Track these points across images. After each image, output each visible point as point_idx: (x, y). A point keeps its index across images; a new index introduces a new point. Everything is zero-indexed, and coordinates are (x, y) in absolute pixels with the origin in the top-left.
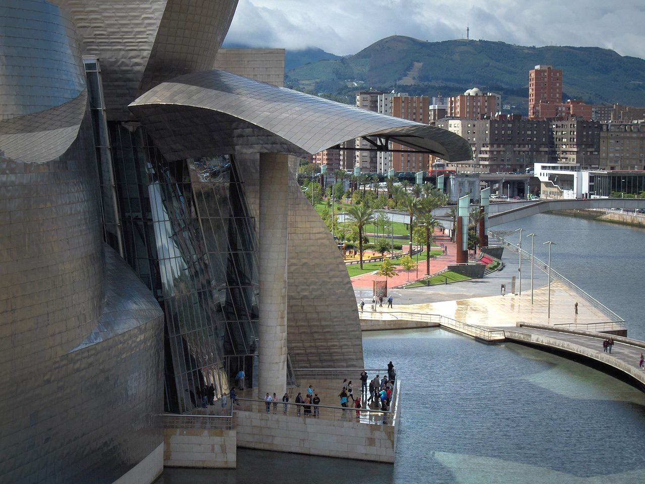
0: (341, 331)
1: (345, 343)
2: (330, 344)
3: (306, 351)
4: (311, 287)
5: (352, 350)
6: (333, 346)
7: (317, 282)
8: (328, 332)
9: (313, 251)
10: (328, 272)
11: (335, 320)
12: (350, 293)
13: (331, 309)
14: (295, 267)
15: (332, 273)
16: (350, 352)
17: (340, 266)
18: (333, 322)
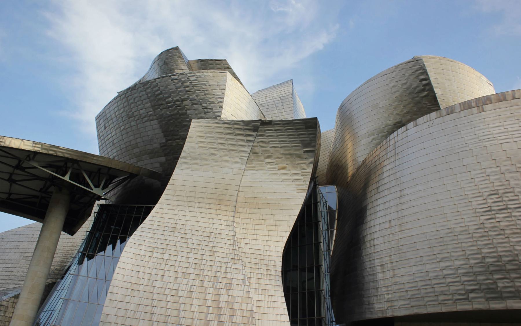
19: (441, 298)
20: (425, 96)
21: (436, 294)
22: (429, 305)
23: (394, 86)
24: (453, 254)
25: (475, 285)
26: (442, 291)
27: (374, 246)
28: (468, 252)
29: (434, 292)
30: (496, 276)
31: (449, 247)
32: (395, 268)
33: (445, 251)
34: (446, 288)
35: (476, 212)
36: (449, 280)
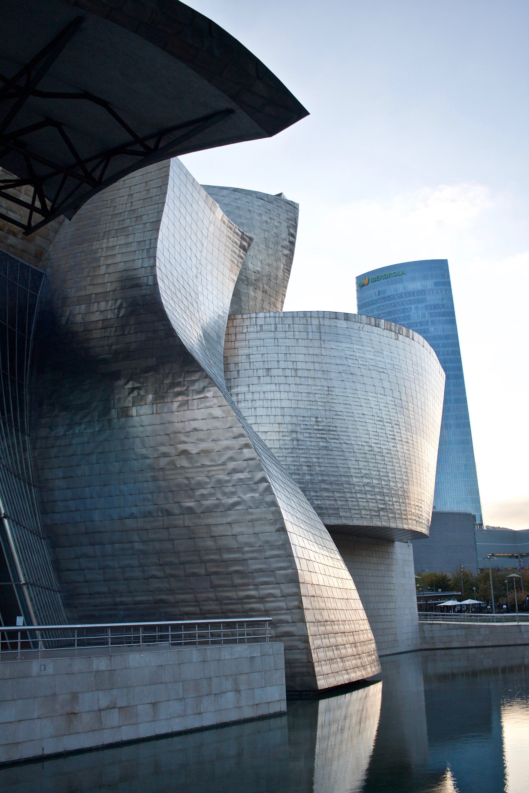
0: (260, 570)
1: (272, 591)
2: (242, 594)
3: (201, 610)
4: (198, 493)
5: (282, 604)
6: (248, 597)
7: (207, 483)
8: (237, 572)
9: (195, 430)
10: (224, 464)
11: (247, 549)
12: (268, 499)
13: (237, 529)
14: (167, 459)
15: (231, 465)
16: (281, 609)
17: (245, 450)
18: (243, 553)
19: (363, 512)
20: (286, 256)
21: (360, 508)
22: (355, 517)
23: (266, 222)
24: (372, 472)
25: (383, 504)
26: (364, 506)
27: (298, 440)
28: (382, 474)
29: (359, 506)
30: (394, 499)
31: (370, 464)
32: (324, 473)
33: (367, 468)
34: (366, 504)
35: (387, 437)
36: (369, 496)
